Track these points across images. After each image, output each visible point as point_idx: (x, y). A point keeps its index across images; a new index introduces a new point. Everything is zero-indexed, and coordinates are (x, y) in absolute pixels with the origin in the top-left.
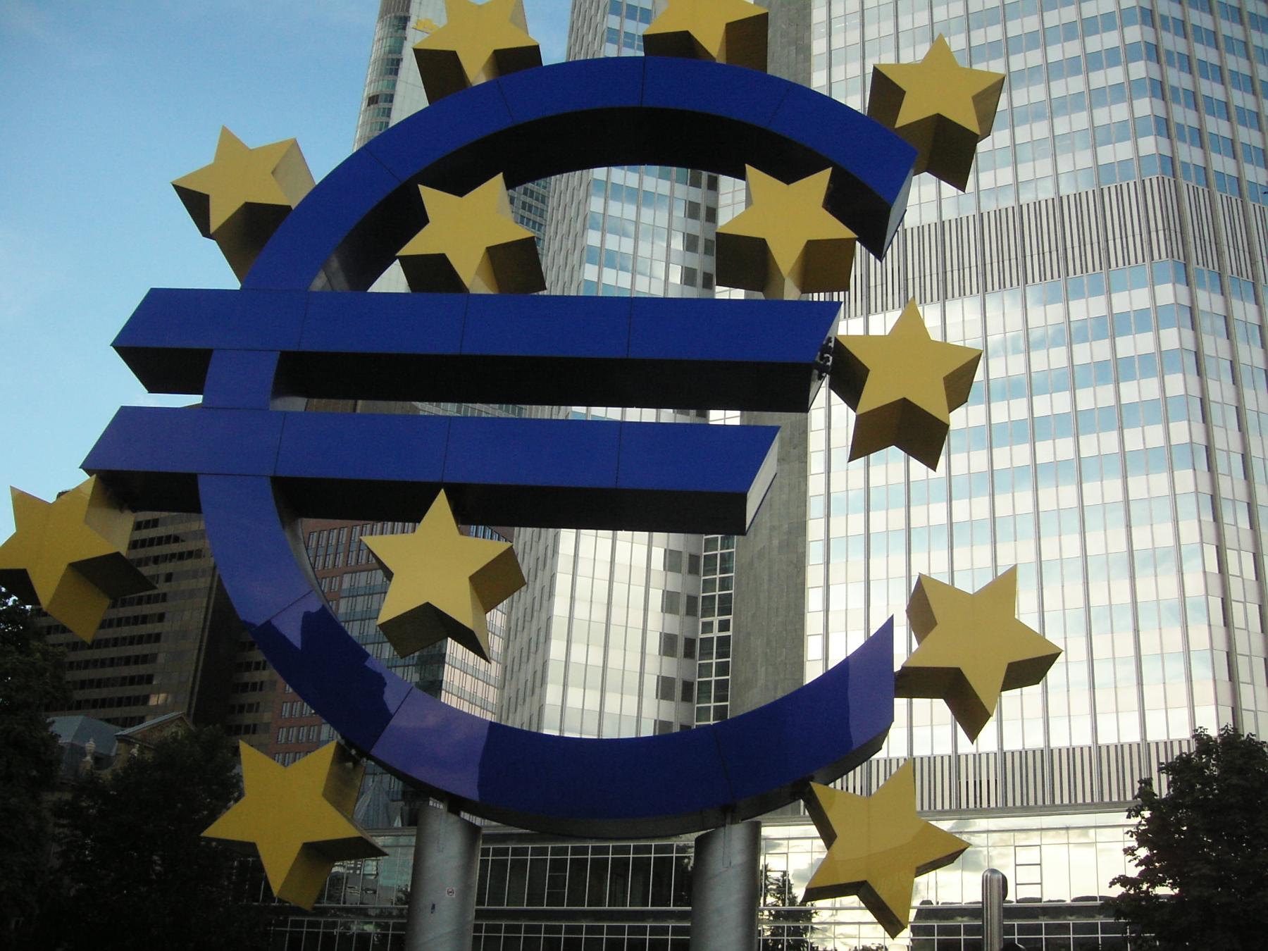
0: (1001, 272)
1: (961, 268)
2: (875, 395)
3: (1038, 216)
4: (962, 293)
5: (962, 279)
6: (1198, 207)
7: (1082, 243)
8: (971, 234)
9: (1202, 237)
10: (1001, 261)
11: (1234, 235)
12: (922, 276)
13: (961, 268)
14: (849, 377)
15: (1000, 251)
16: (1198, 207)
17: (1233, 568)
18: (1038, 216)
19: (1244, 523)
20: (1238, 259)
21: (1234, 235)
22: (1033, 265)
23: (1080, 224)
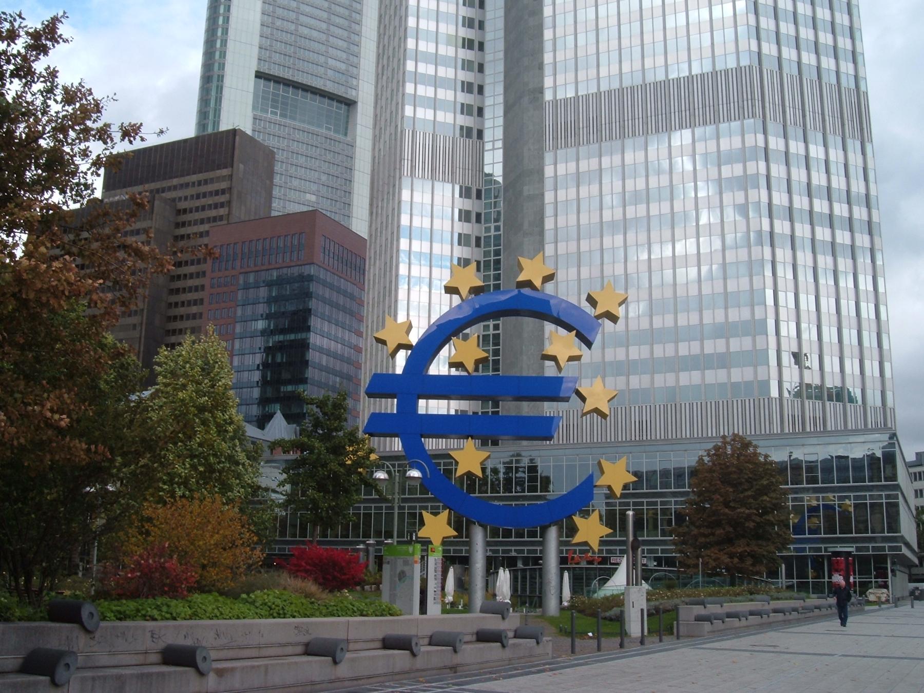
0: (657, 122)
1: (633, 119)
2: (588, 406)
3: (679, 87)
4: (634, 135)
5: (634, 126)
6: (773, 83)
7: (704, 106)
8: (638, 96)
9: (774, 103)
10: (656, 115)
11: (793, 99)
12: (610, 123)
13: (633, 119)
14: (583, 399)
15: (656, 109)
16: (773, 83)
17: (781, 301)
18: (679, 87)
19: (790, 276)
20: (795, 115)
21: (793, 99)
22: (675, 119)
23: (703, 93)
